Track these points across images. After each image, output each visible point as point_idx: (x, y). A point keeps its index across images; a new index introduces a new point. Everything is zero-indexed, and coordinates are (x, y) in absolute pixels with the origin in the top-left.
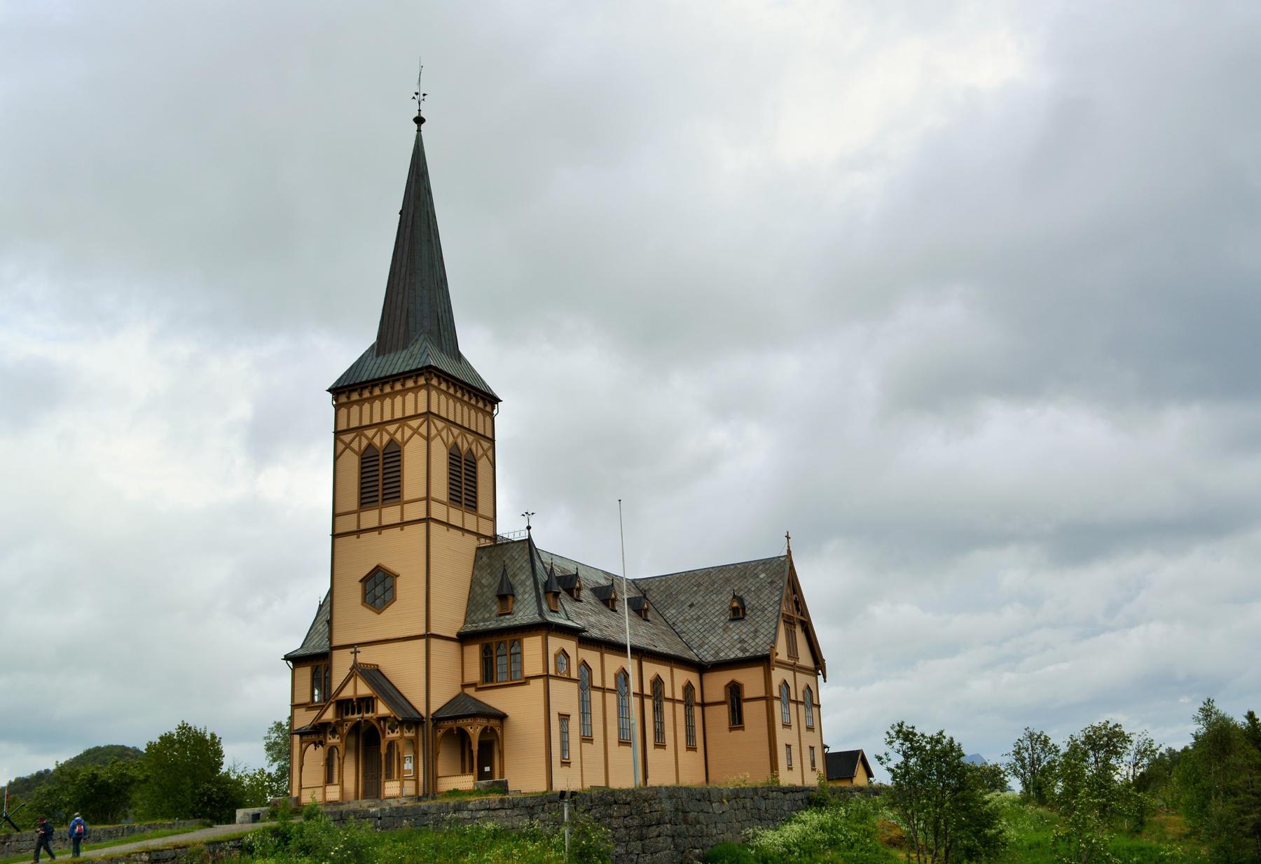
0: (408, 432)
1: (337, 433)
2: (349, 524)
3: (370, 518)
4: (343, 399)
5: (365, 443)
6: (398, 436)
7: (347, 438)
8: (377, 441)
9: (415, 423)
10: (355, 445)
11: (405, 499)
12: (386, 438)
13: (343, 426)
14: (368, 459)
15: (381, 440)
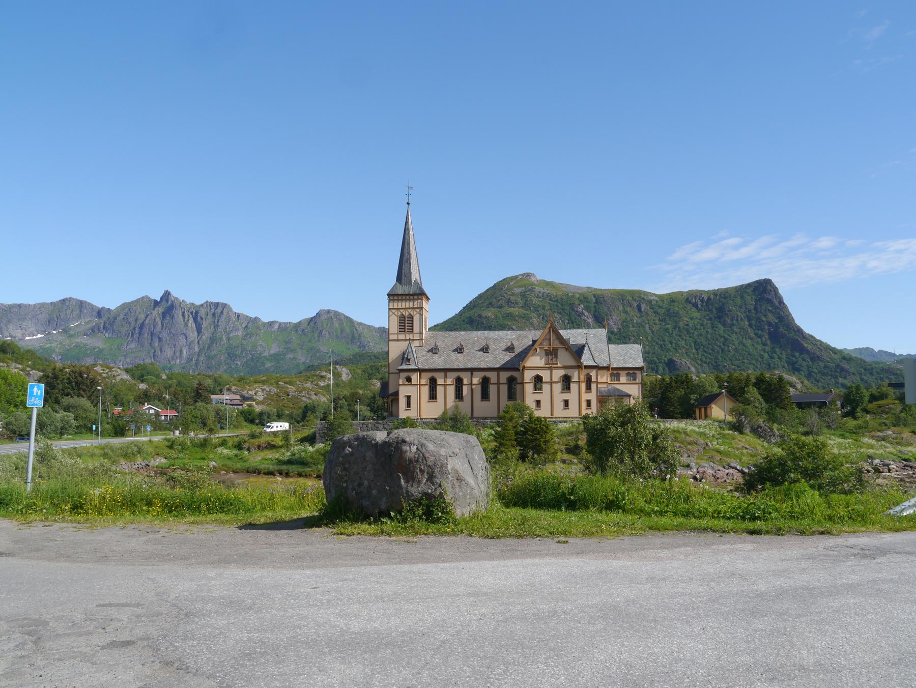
0: (415, 313)
1: (390, 309)
2: (395, 337)
3: (402, 337)
4: (391, 298)
5: (400, 313)
6: (412, 313)
7: (394, 311)
8: (404, 313)
9: (418, 310)
10: (396, 313)
11: (414, 332)
12: (407, 313)
13: (391, 307)
14: (402, 319)
15: (406, 313)
